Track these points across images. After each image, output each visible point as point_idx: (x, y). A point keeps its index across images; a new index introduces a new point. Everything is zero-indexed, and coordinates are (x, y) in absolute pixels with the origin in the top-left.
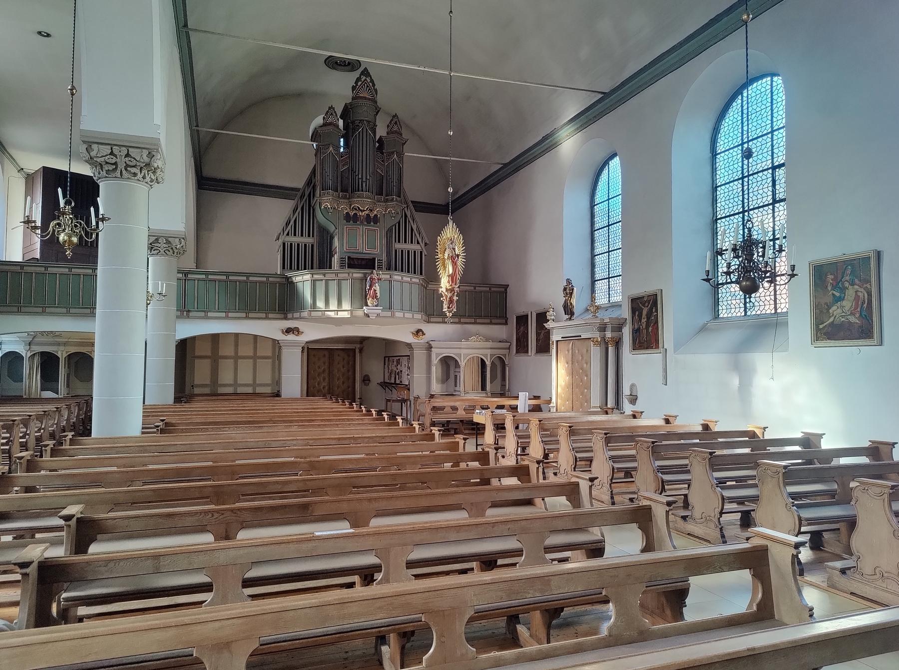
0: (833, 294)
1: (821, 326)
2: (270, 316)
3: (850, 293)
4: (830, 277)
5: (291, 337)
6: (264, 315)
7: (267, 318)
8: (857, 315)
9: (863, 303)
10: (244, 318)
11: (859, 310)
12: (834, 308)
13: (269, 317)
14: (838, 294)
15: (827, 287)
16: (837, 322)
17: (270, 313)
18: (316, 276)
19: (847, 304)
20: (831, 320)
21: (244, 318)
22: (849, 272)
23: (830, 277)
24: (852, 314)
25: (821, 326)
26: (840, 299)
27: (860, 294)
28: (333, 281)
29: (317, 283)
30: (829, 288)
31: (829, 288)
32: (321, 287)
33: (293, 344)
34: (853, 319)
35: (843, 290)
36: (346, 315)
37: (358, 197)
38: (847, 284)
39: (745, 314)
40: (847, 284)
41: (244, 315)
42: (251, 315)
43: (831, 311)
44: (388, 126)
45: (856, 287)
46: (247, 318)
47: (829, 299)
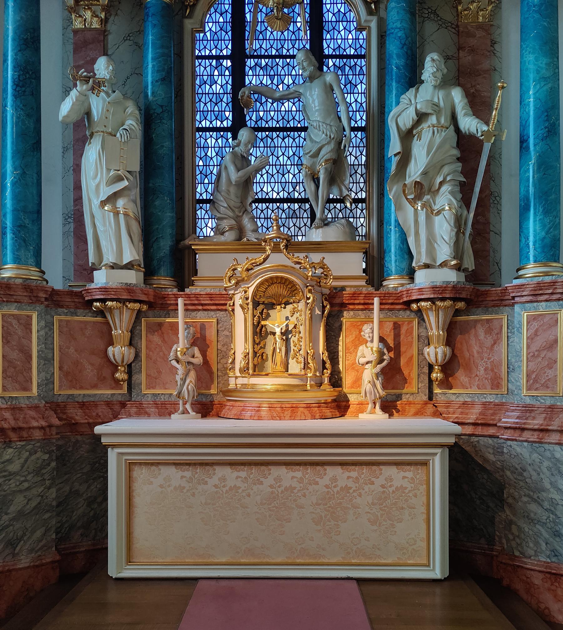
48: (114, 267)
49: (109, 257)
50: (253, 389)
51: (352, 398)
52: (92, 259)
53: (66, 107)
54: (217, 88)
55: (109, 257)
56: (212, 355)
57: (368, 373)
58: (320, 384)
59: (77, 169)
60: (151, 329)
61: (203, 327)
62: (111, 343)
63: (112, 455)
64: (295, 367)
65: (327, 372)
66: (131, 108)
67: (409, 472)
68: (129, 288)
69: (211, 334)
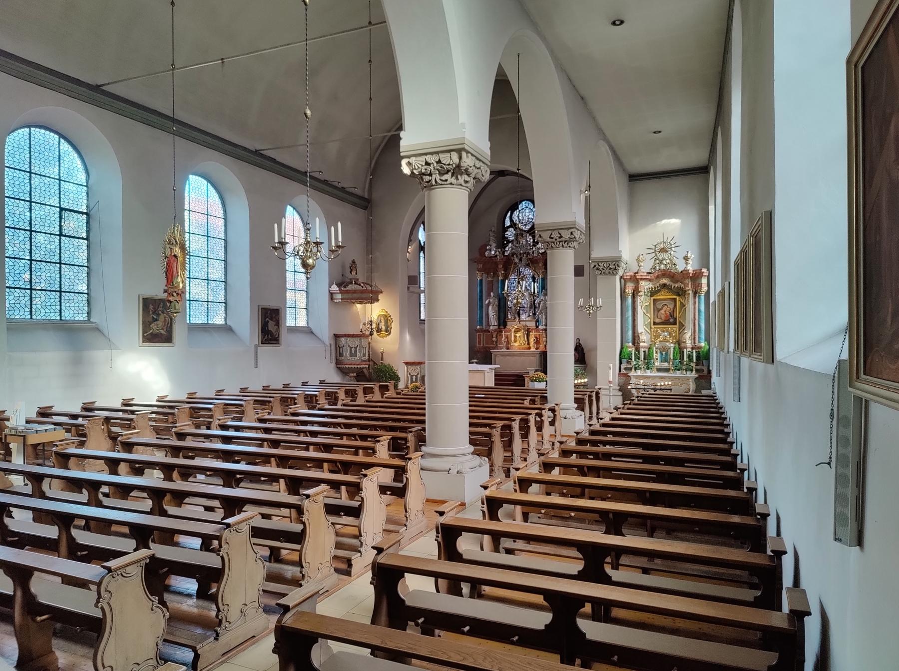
0: (153, 317)
1: (145, 335)
3: (162, 317)
4: (151, 307)
8: (165, 330)
9: (168, 324)
11: (166, 327)
12: (153, 324)
14: (155, 317)
15: (149, 312)
16: (154, 333)
19: (160, 323)
20: (151, 331)
22: (161, 306)
23: (151, 307)
24: (162, 329)
25: (145, 335)
26: (156, 320)
27: (167, 319)
30: (151, 313)
31: (151, 313)
34: (162, 332)
35: (158, 315)
38: (160, 312)
39: (31, 318)
40: (160, 312)
43: (151, 326)
45: (165, 314)
47: (150, 319)
48: (493, 326)
49: (493, 324)
50: (514, 345)
51: (532, 347)
52: (490, 324)
53: (487, 302)
54: (514, 285)
55: (493, 324)
56: (509, 340)
57: (533, 343)
58: (525, 344)
59: (488, 309)
60: (499, 336)
61: (508, 335)
62: (493, 338)
63: (493, 354)
64: (521, 342)
65: (527, 343)
66: (496, 300)
67: (534, 357)
68: (495, 329)
69: (509, 336)
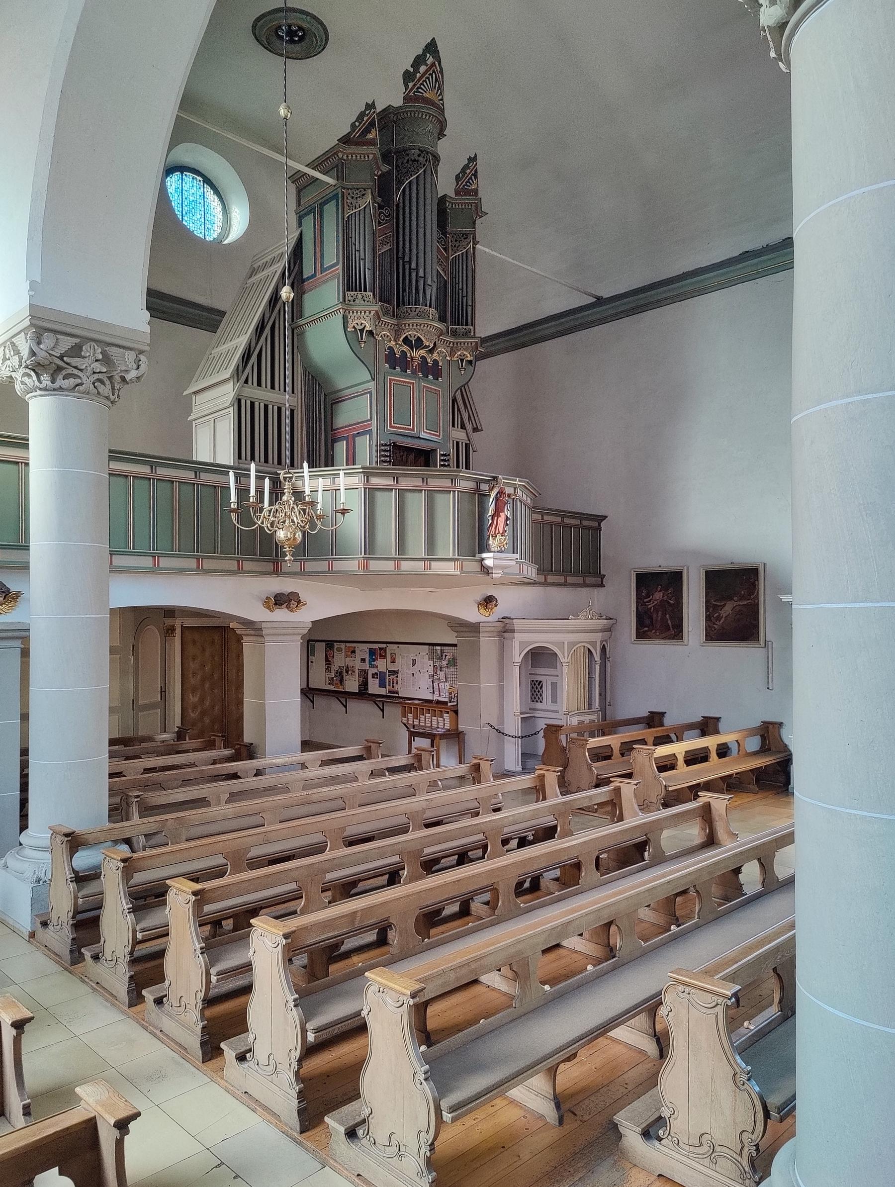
2: (247, 566)
5: (281, 615)
6: (233, 565)
7: (240, 571)
10: (193, 570)
13: (245, 569)
17: (247, 559)
18: (375, 481)
21: (193, 570)
28: (416, 495)
29: (379, 496)
32: (387, 505)
33: (283, 630)
36: (449, 568)
37: (419, 316)
41: (192, 563)
42: (207, 564)
44: (458, 178)
46: (199, 570)
